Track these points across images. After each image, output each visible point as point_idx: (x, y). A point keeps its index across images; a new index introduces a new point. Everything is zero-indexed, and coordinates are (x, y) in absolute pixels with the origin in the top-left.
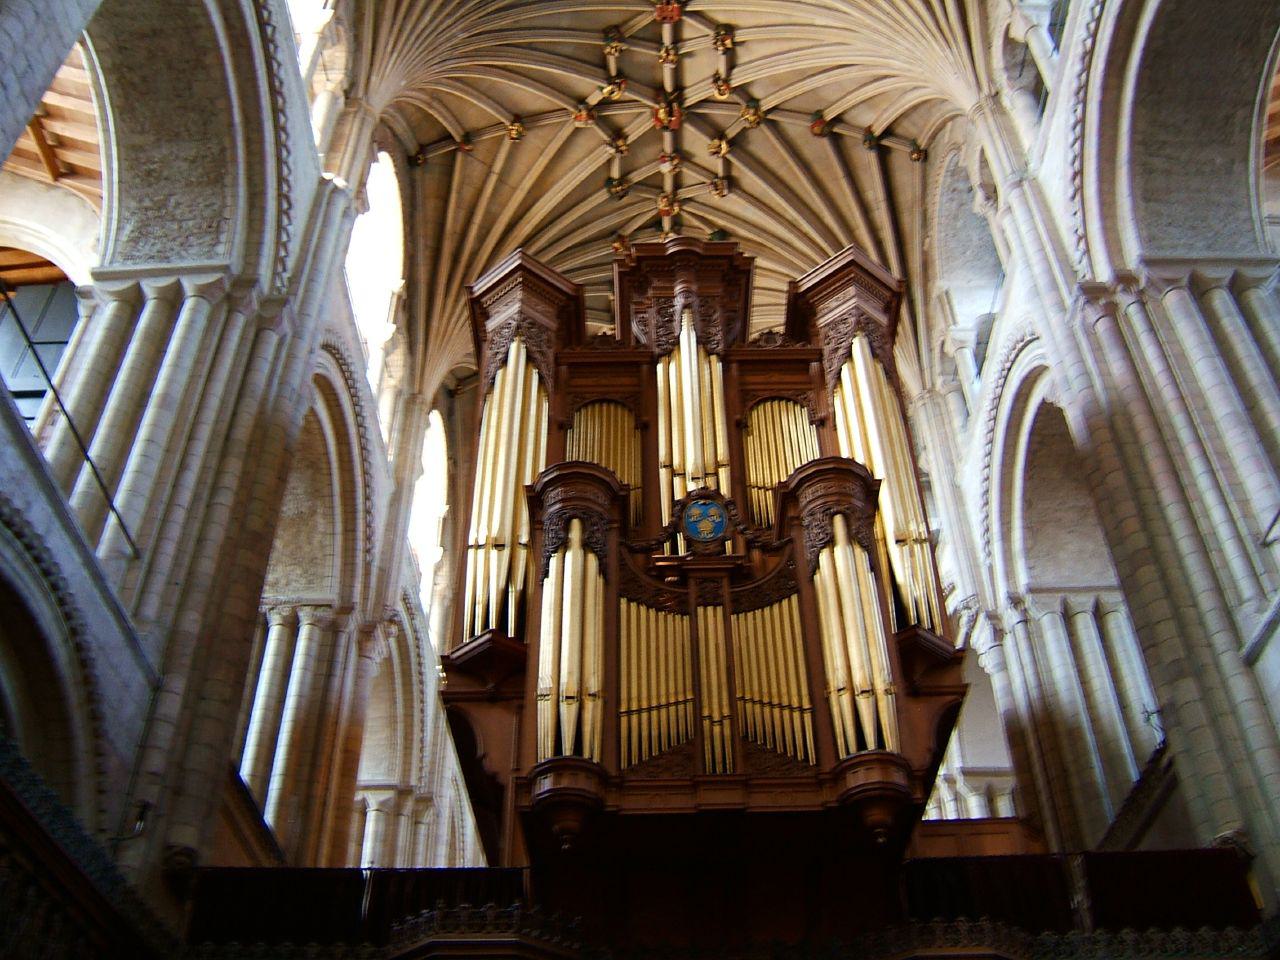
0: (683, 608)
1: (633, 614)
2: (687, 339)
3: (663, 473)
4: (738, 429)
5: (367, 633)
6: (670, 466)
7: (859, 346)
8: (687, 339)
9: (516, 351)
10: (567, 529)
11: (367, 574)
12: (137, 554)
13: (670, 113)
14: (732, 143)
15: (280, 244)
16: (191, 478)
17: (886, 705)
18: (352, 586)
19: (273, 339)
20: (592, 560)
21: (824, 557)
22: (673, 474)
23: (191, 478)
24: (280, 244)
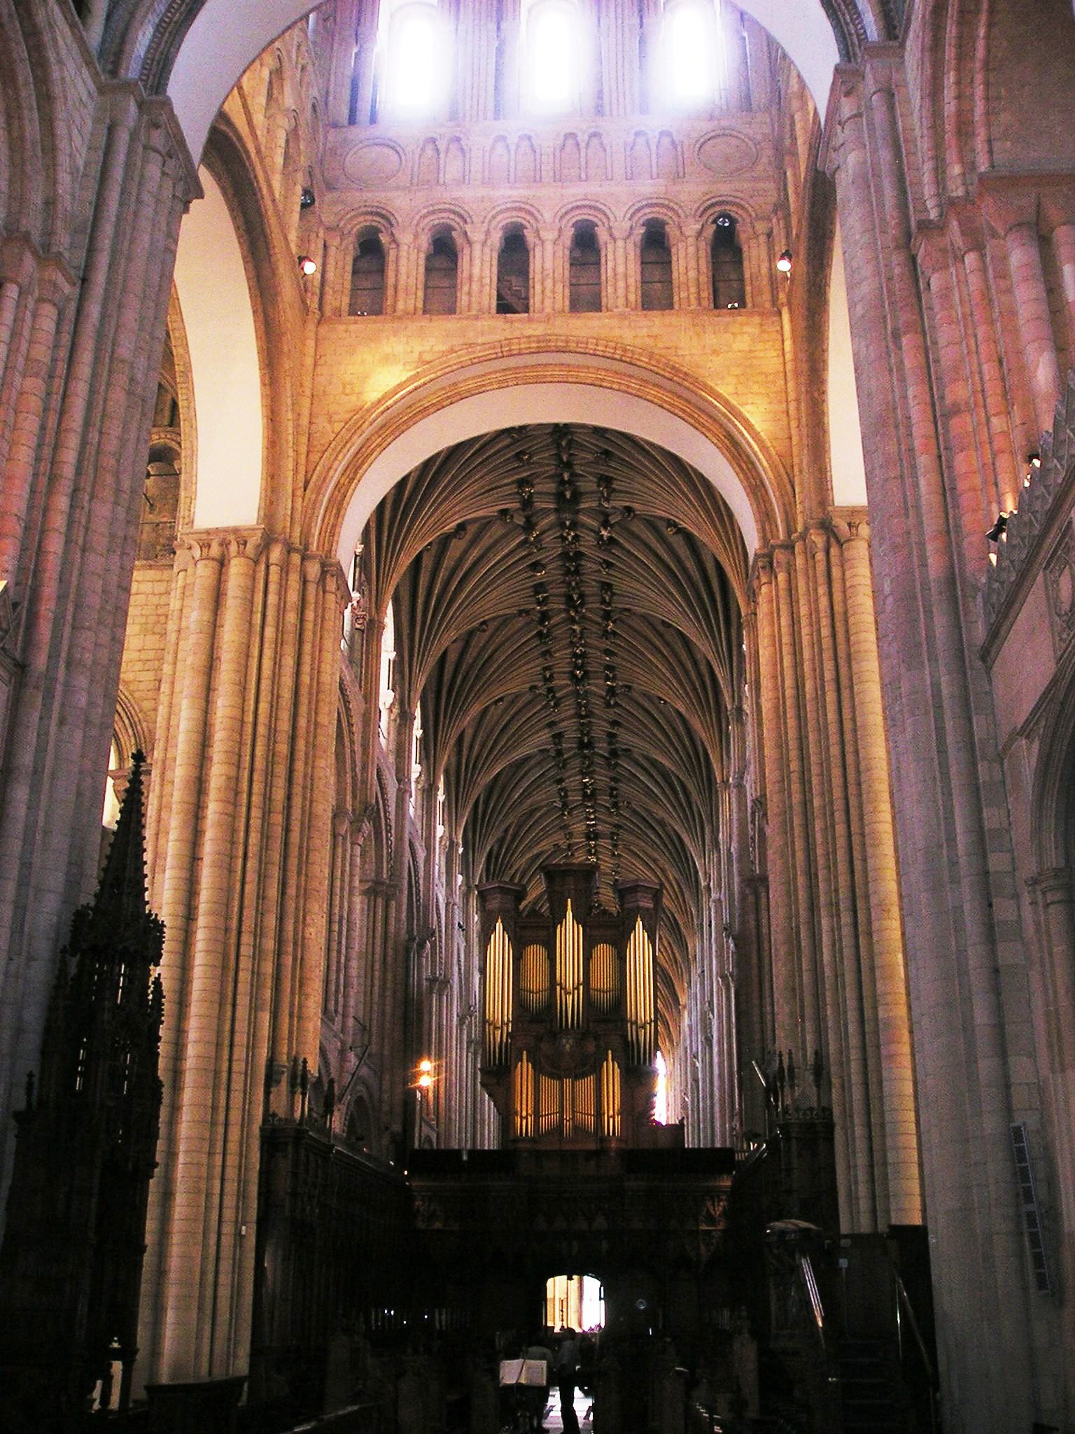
0: (560, 1078)
1: (545, 1082)
2: (569, 914)
3: (558, 988)
4: (588, 958)
5: (421, 946)
6: (561, 984)
7: (639, 924)
8: (569, 914)
9: (499, 926)
10: (522, 1054)
11: (418, 912)
12: (365, 1028)
13: (577, 612)
14: (613, 622)
15: (389, 847)
16: (376, 988)
17: (618, 1119)
18: (412, 925)
19: (393, 903)
20: (530, 1065)
21: (605, 1064)
22: (561, 989)
23: (376, 988)
24: (389, 847)
